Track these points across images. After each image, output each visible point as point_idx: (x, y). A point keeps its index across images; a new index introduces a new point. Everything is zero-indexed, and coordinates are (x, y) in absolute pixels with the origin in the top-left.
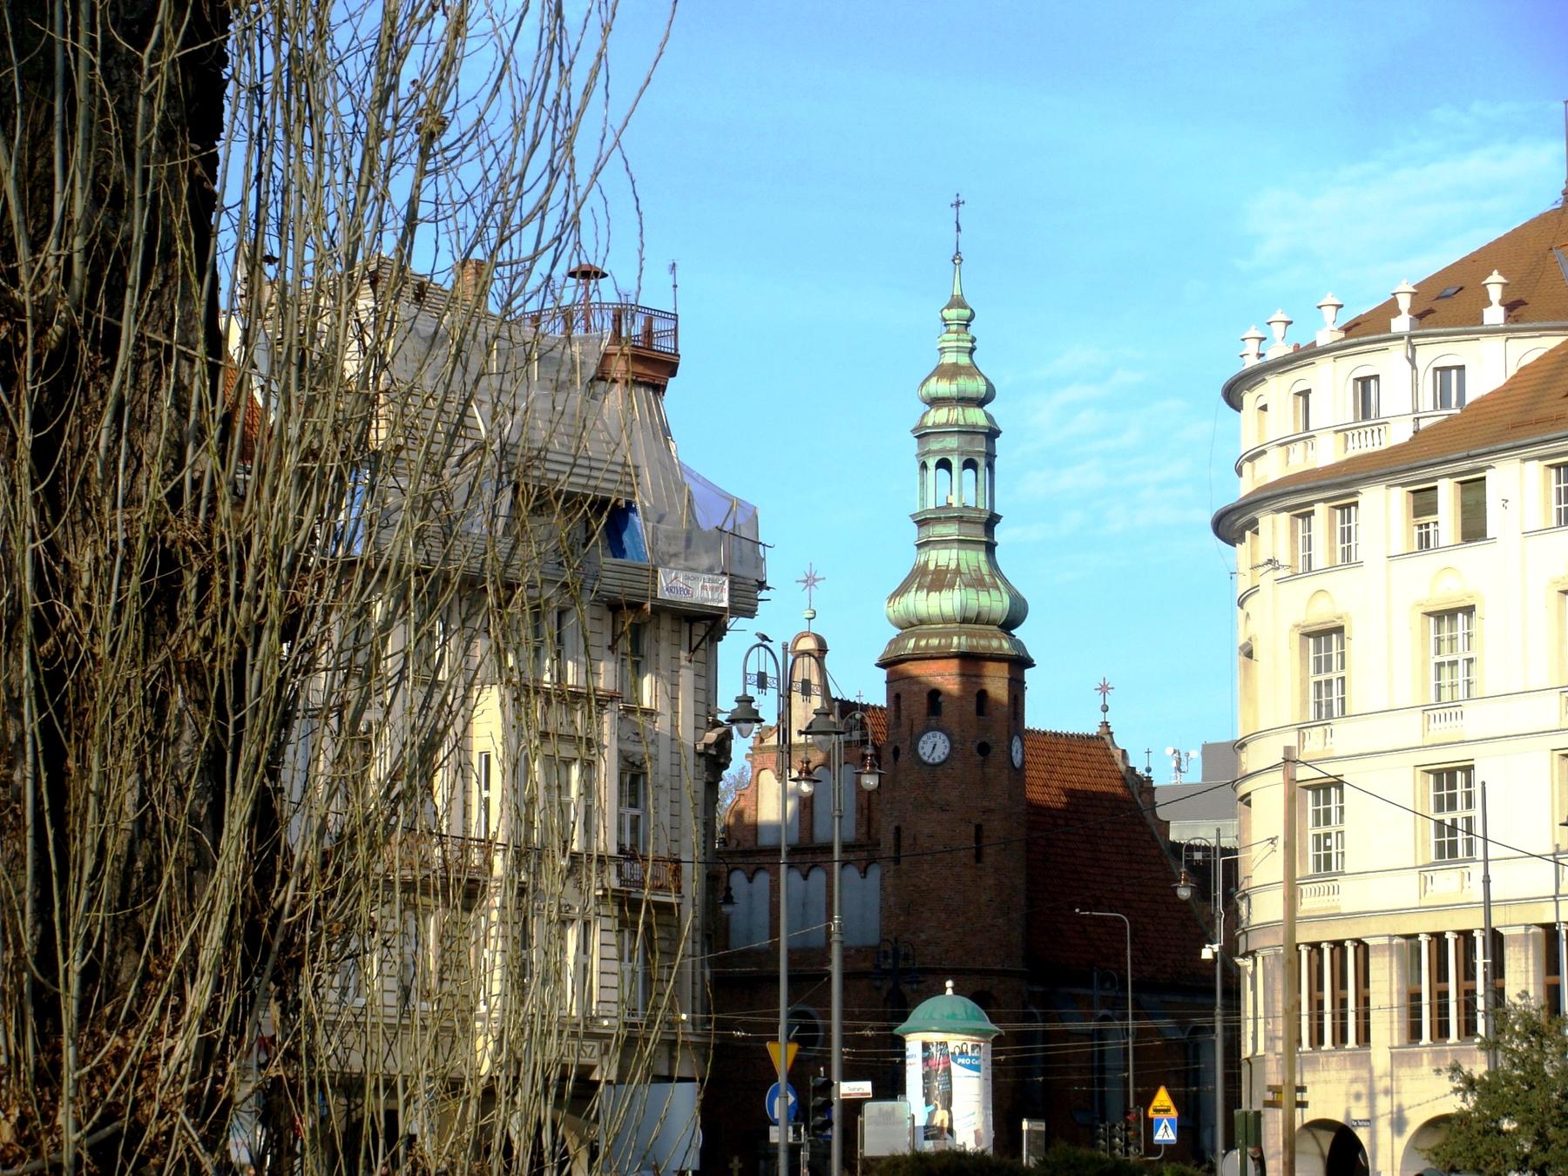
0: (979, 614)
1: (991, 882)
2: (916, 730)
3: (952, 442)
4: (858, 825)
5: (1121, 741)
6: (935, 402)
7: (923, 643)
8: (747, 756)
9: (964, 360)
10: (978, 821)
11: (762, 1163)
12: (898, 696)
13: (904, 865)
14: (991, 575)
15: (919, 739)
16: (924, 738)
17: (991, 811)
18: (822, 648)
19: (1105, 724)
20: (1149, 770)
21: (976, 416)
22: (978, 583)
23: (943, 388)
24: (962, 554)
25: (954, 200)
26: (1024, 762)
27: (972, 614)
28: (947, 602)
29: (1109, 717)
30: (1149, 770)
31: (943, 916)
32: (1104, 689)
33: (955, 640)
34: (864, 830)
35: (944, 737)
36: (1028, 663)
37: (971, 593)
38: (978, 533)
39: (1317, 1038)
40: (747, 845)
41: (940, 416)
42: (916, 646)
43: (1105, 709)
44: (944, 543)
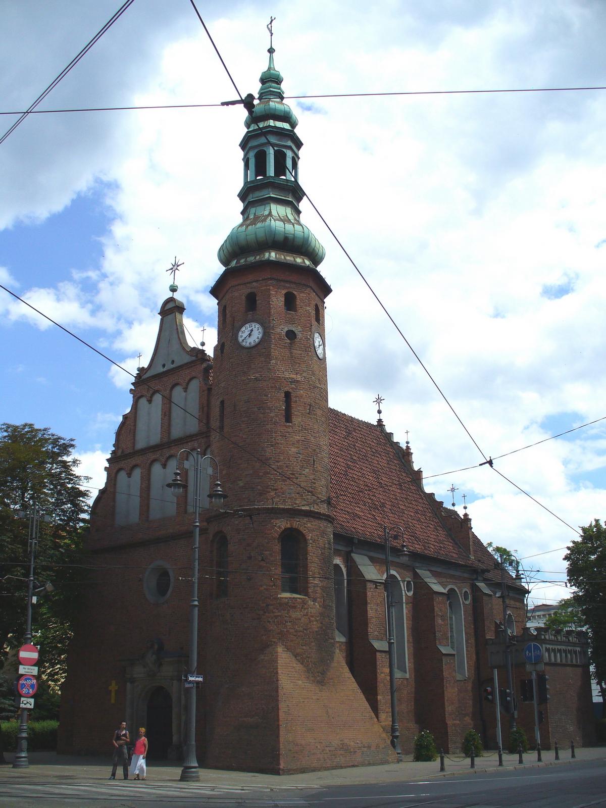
8: (131, 390)
10: (286, 389)
11: (129, 685)
12: (225, 307)
13: (226, 430)
14: (295, 219)
16: (243, 329)
17: (298, 382)
19: (380, 421)
20: (408, 443)
22: (286, 220)
29: (382, 416)
30: (408, 443)
32: (379, 401)
33: (267, 255)
35: (257, 326)
36: (327, 290)
42: (236, 263)
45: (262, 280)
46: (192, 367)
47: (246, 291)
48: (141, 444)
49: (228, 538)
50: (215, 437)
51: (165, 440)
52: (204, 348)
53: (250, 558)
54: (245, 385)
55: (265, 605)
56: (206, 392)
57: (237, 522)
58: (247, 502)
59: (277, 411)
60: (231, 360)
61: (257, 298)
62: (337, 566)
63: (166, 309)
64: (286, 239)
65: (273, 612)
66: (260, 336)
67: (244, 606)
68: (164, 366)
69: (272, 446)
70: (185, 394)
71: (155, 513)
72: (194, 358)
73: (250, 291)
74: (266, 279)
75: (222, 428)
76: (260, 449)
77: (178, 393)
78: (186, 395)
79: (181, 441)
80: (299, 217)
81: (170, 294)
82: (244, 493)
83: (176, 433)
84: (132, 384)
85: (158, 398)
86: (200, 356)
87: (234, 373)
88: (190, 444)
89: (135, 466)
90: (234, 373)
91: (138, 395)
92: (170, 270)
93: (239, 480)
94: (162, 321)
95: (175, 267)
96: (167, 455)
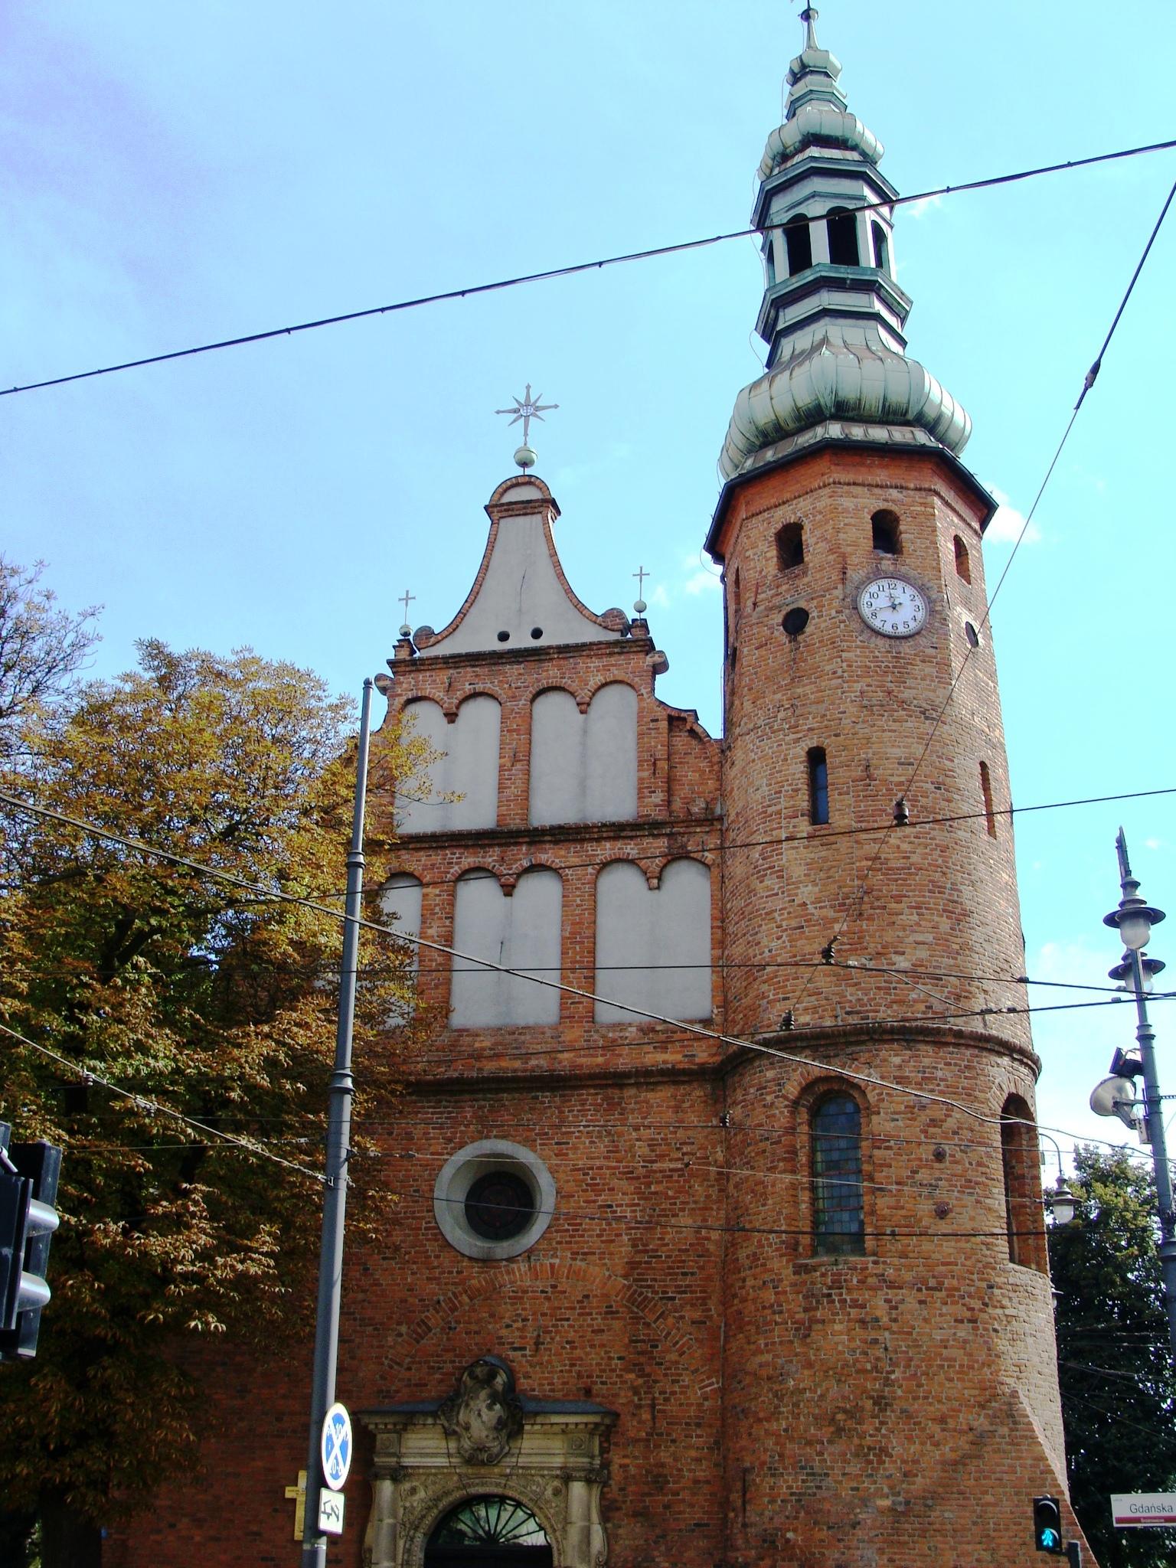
2: (855, 575)
4: (643, 791)
15: (860, 587)
16: (873, 588)
34: (658, 797)
35: (910, 591)
45: (916, 489)
46: (611, 654)
47: (873, 502)
49: (872, 1097)
51: (515, 823)
52: (643, 615)
53: (939, 1156)
54: (894, 721)
55: (984, 1285)
56: (664, 725)
57: (897, 1060)
58: (924, 1013)
59: (971, 801)
60: (844, 655)
61: (902, 528)
63: (506, 499)
64: (939, 419)
65: (1003, 1307)
66: (920, 615)
67: (932, 1283)
68: (504, 637)
69: (973, 884)
72: (615, 636)
73: (883, 505)
74: (925, 490)
76: (949, 886)
78: (586, 720)
81: (519, 471)
82: (913, 989)
83: (550, 807)
84: (390, 663)
85: (482, 716)
86: (638, 633)
87: (858, 687)
88: (608, 845)
90: (858, 687)
92: (509, 411)
93: (896, 953)
95: (526, 410)
96: (526, 863)
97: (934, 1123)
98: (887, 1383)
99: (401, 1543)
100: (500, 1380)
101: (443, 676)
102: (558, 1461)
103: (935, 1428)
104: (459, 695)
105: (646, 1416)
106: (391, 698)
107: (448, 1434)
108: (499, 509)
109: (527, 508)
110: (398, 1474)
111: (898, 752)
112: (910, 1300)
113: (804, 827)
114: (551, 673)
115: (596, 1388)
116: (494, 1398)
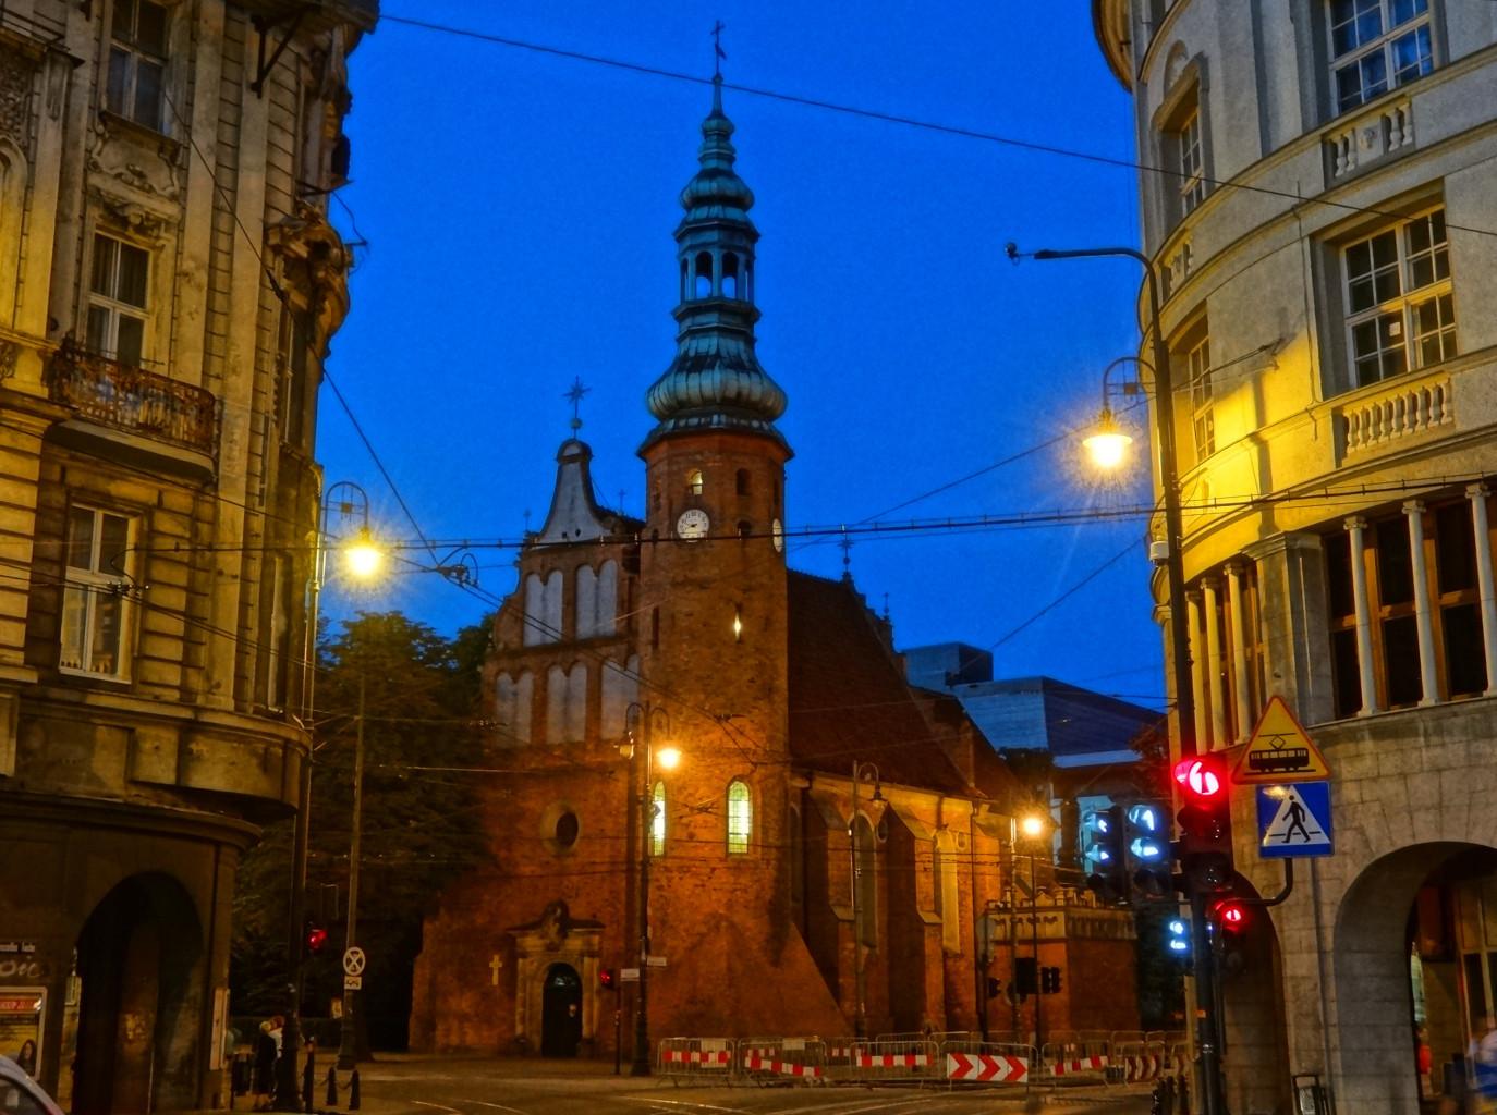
0: (739, 394)
1: (752, 662)
3: (714, 236)
5: (860, 586)
6: (698, 201)
7: (682, 423)
9: (723, 165)
11: (520, 961)
13: (662, 647)
16: (684, 517)
18: (586, 453)
19: (847, 575)
20: (886, 610)
21: (733, 213)
23: (708, 187)
24: (722, 341)
25: (713, 28)
26: (784, 550)
27: (732, 393)
28: (708, 383)
29: (851, 568)
30: (886, 610)
31: (702, 697)
33: (715, 418)
35: (703, 515)
36: (789, 454)
37: (731, 375)
38: (735, 322)
39: (1401, 686)
40: (513, 646)
41: (702, 213)
43: (847, 561)
44: (705, 332)
48: (533, 637)
50: (645, 650)
62: (793, 810)
64: (739, 394)
66: (706, 529)
70: (595, 579)
71: (554, 735)
75: (655, 643)
77: (586, 576)
79: (590, 644)
80: (752, 331)
81: (568, 434)
83: (585, 628)
85: (557, 579)
89: (523, 669)
91: (526, 571)
94: (560, 469)
95: (577, 393)
97: (690, 795)
98: (666, 914)
99: (528, 985)
100: (559, 912)
101: (539, 560)
102: (579, 948)
103: (684, 934)
104: (546, 570)
105: (615, 926)
106: (520, 572)
107: (542, 937)
108: (563, 459)
109: (572, 459)
110: (524, 955)
111: (686, 610)
112: (676, 875)
113: (650, 648)
114: (583, 555)
115: (599, 915)
116: (556, 921)
